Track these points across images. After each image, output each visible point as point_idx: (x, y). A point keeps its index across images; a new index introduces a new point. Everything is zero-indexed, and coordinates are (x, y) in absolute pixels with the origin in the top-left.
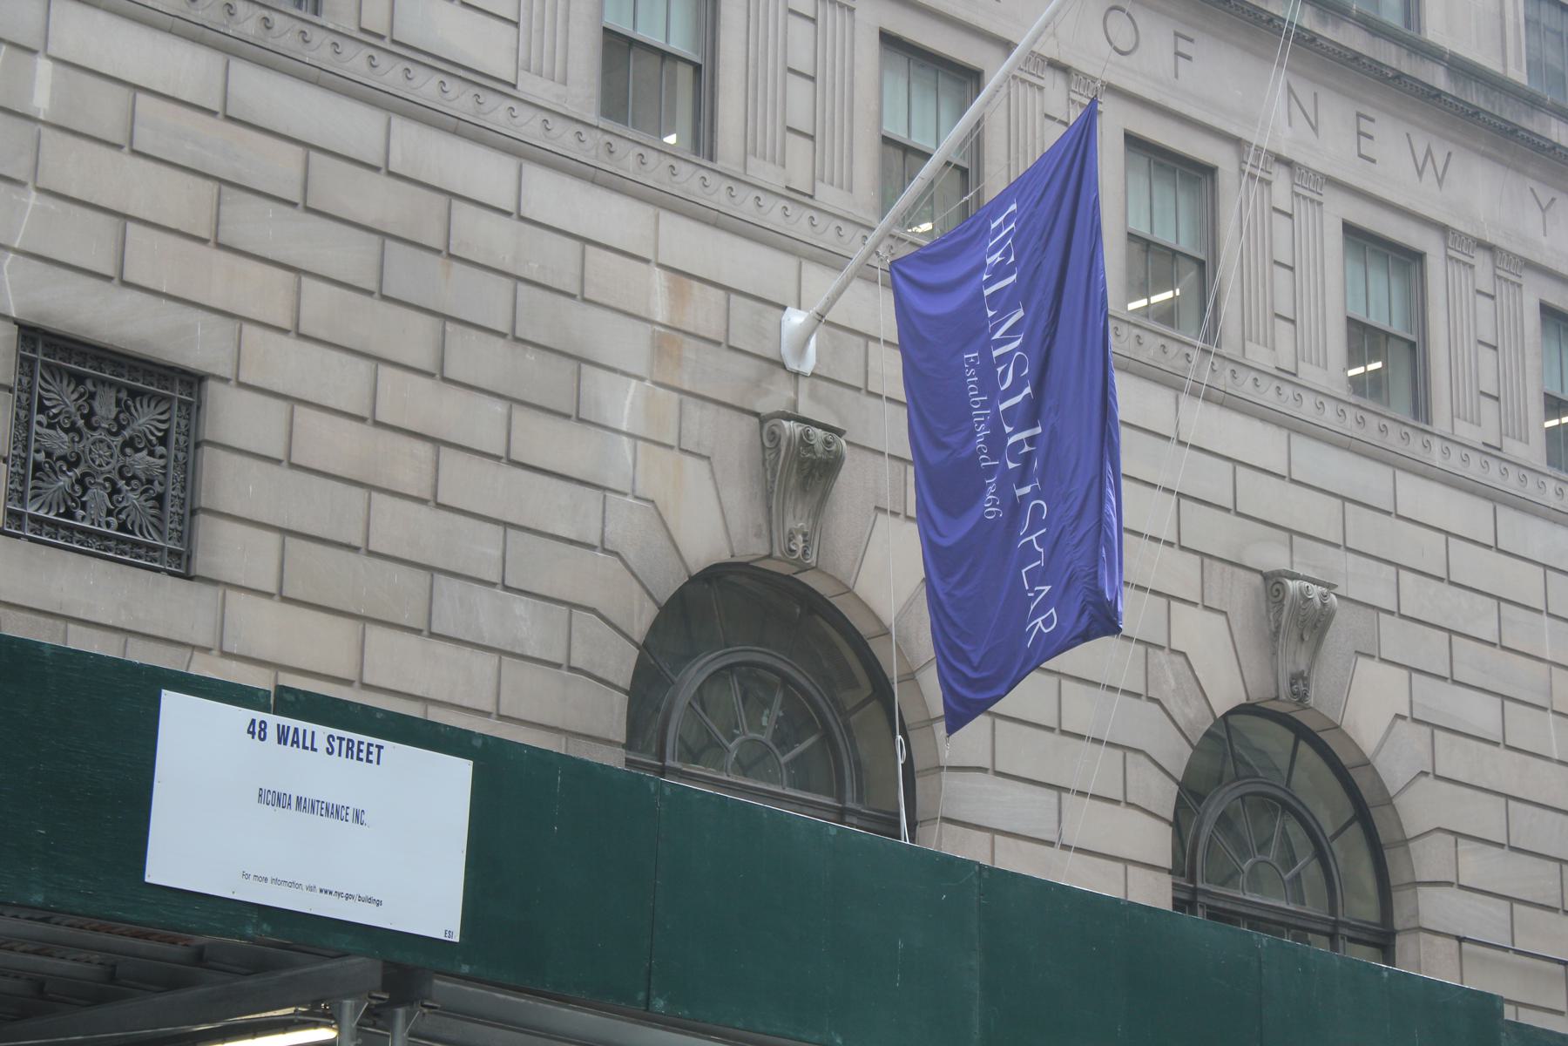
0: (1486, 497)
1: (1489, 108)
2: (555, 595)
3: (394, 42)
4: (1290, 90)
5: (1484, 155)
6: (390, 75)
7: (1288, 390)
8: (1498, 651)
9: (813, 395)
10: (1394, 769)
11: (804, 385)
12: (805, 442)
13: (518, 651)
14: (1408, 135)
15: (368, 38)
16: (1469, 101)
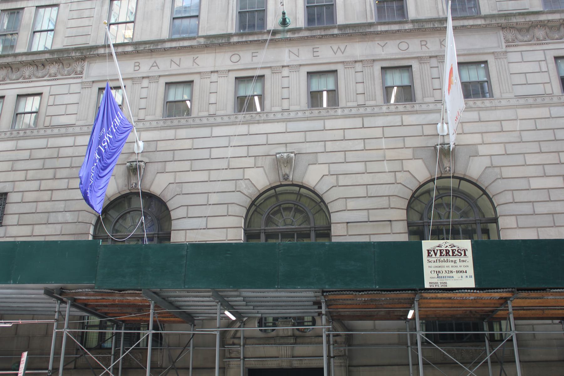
0: (360, 117)
1: (354, 32)
2: (76, 210)
3: (51, 126)
4: (289, 51)
5: (359, 42)
6: (49, 132)
7: (286, 114)
8: (364, 151)
9: (142, 156)
10: (321, 190)
11: (140, 155)
12: (131, 166)
13: (67, 222)
14: (331, 47)
15: (46, 127)
16: (346, 32)
